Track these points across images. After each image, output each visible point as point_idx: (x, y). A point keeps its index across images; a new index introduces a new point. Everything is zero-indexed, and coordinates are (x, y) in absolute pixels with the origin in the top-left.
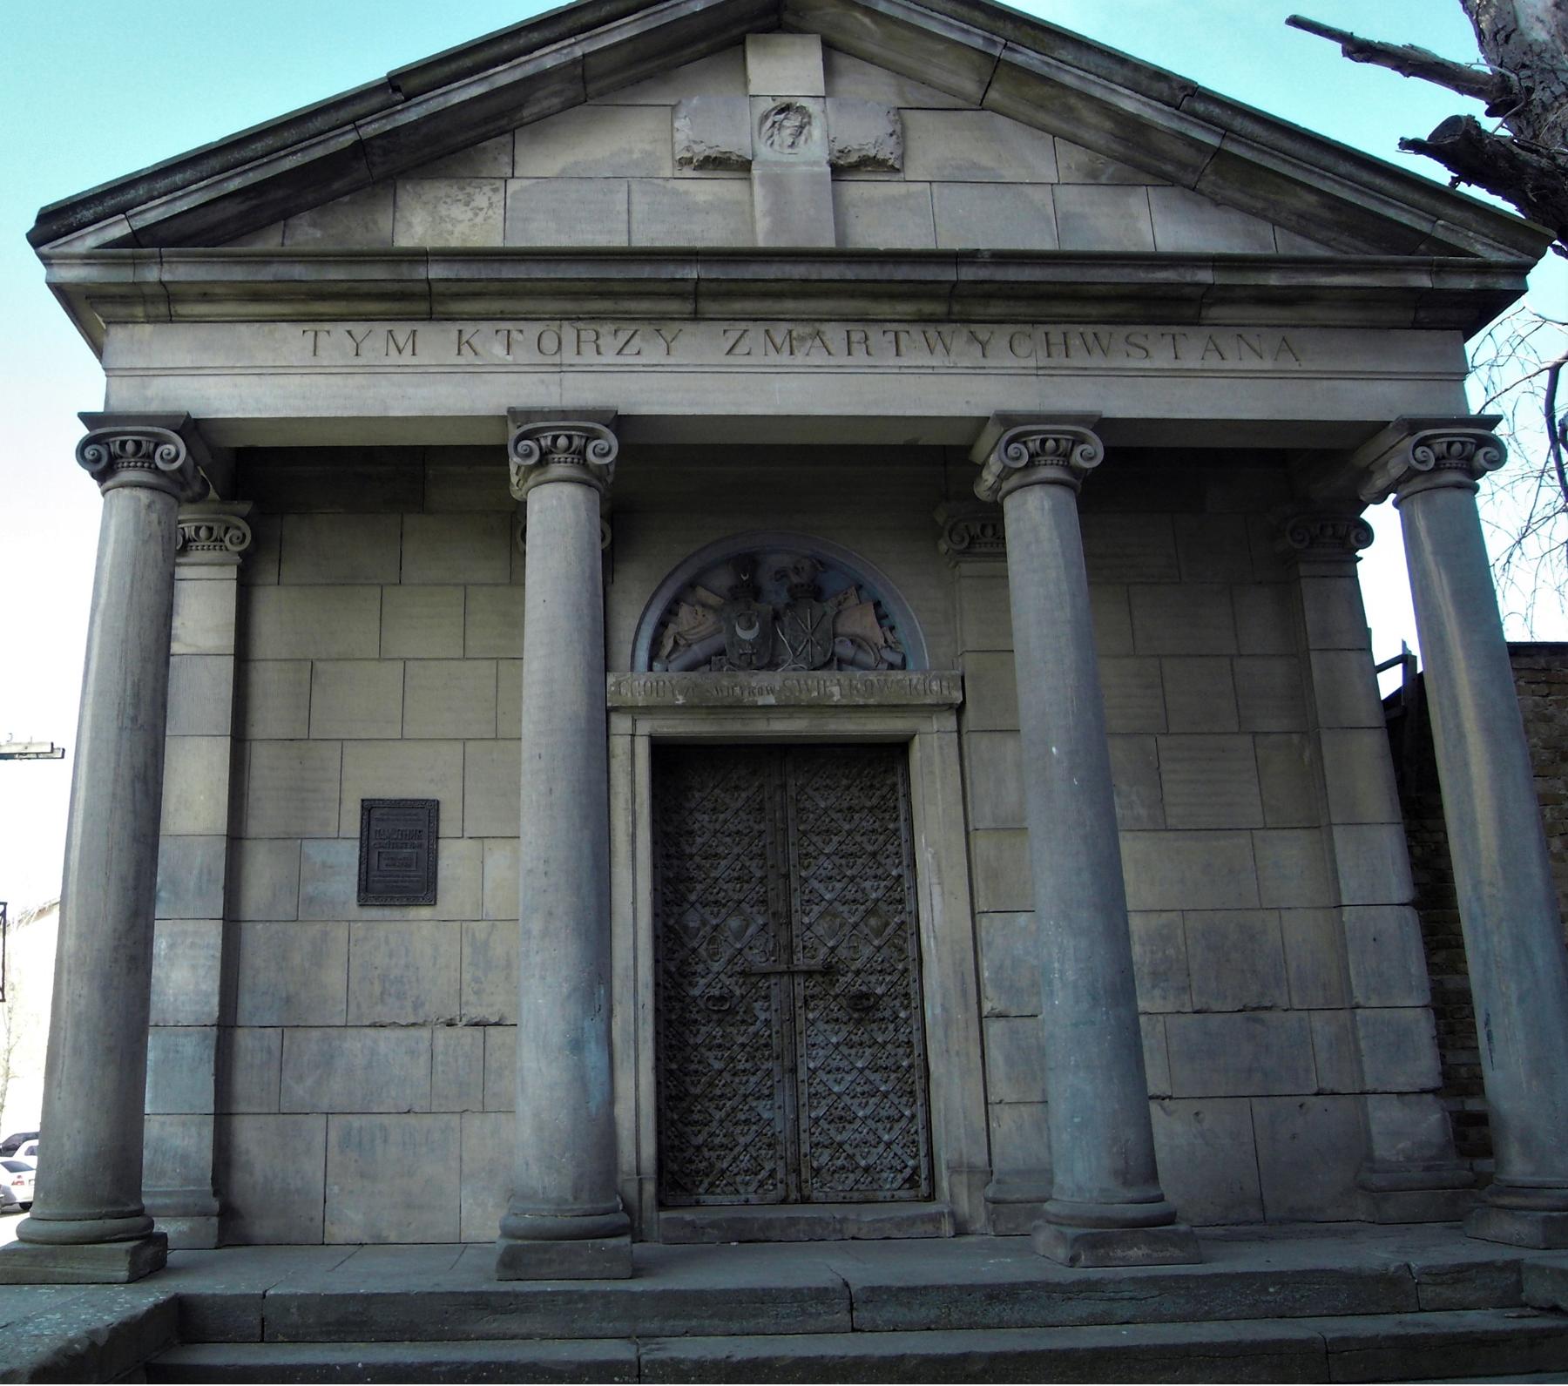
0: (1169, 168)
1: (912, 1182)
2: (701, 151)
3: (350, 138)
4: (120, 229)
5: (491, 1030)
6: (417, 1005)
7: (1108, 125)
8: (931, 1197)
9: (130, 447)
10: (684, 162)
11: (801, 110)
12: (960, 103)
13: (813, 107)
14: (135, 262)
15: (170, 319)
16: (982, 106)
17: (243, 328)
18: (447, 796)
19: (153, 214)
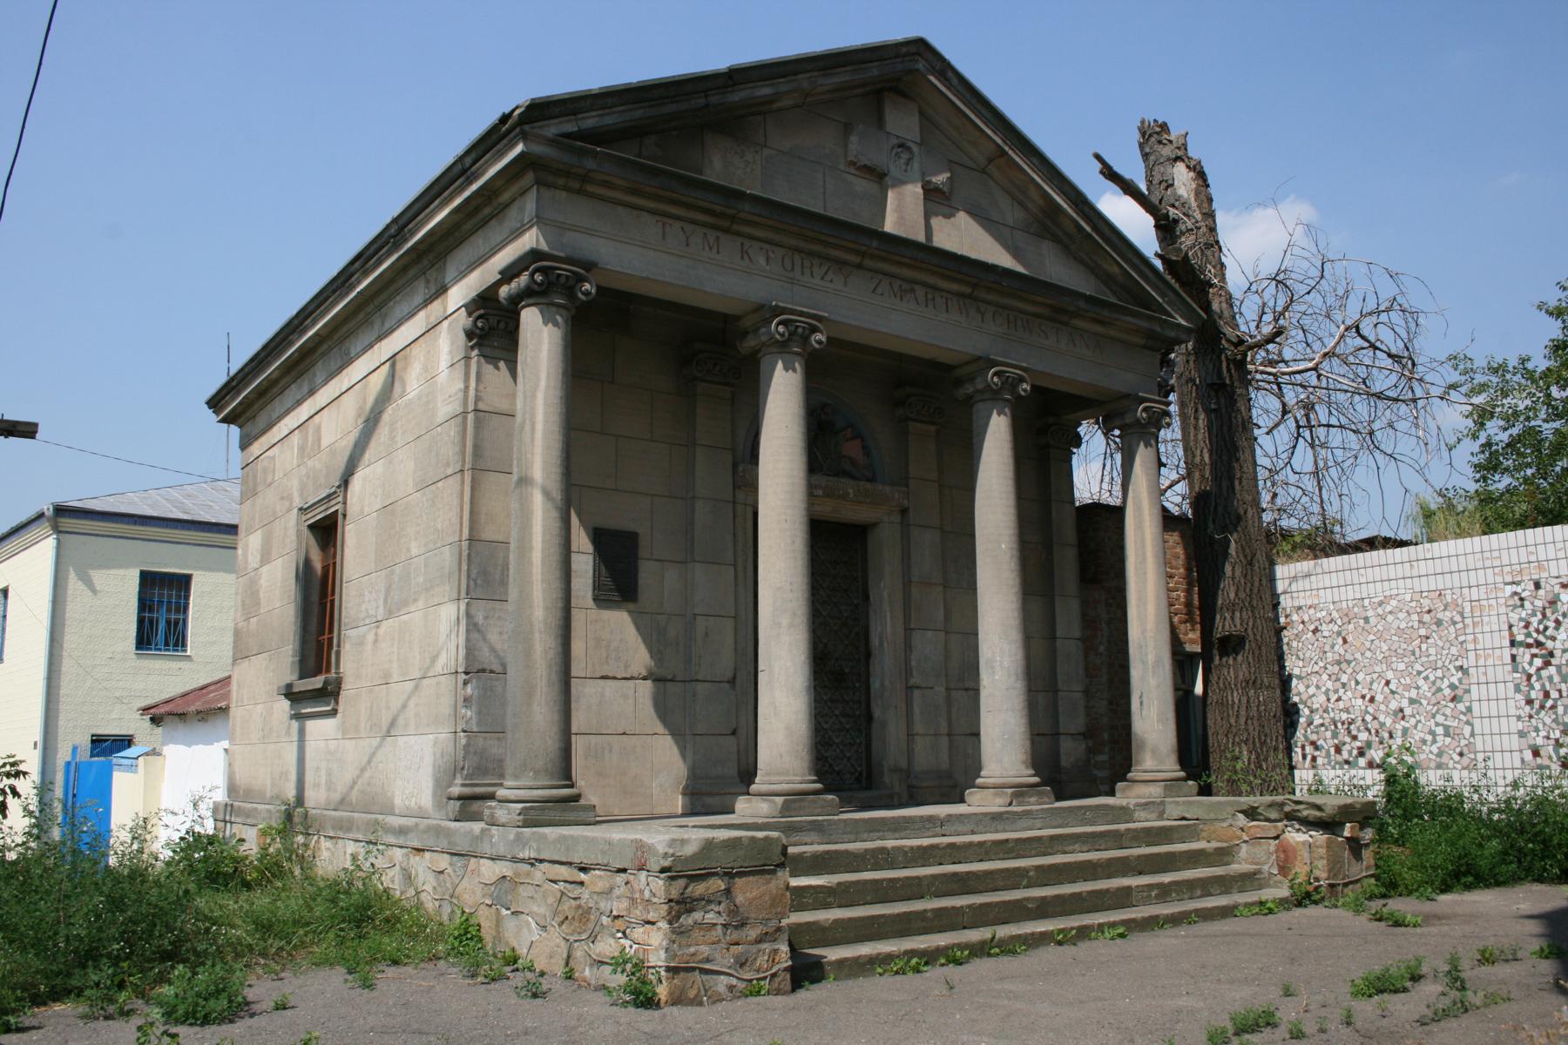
0: (1060, 233)
1: (858, 780)
2: (864, 161)
3: (702, 101)
4: (570, 127)
5: (669, 684)
6: (626, 667)
7: (1041, 202)
8: (869, 787)
9: (563, 280)
10: (853, 164)
11: (909, 149)
12: (971, 164)
13: (915, 149)
14: (582, 153)
15: (579, 192)
16: (983, 172)
17: (620, 209)
18: (640, 531)
19: (590, 121)
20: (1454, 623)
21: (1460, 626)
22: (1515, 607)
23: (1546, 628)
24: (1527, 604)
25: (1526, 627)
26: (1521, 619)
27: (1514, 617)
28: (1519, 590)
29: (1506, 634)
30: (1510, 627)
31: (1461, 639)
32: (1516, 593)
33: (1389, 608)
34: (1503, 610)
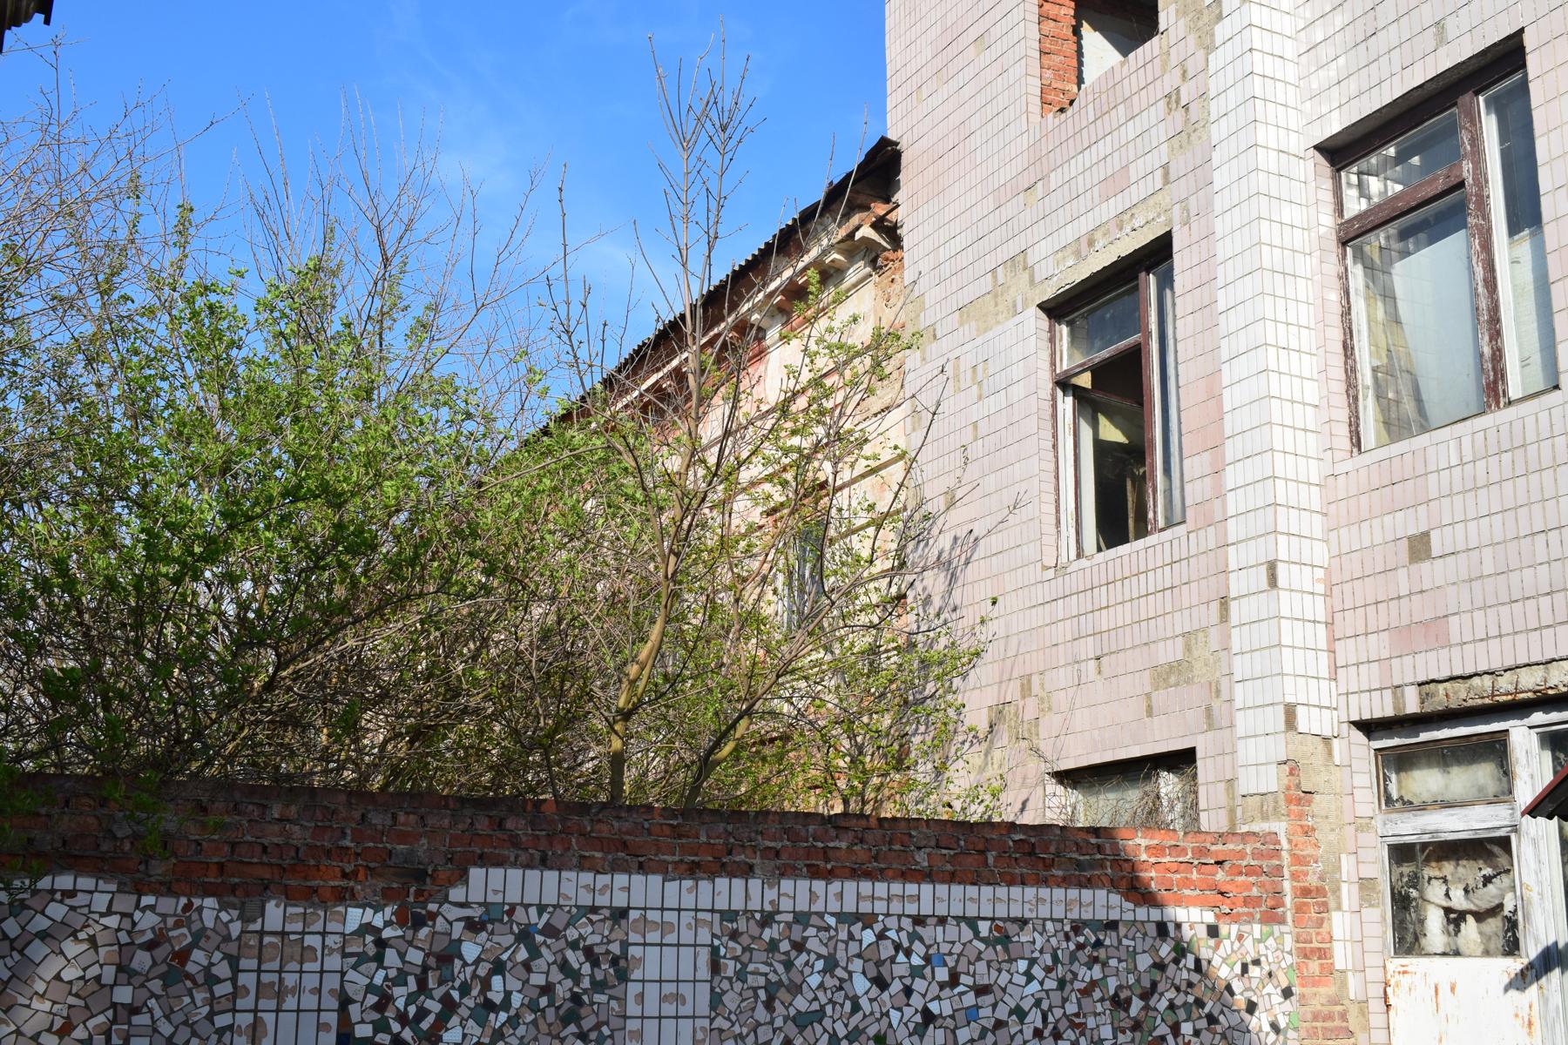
20: (211, 980)
21: (223, 989)
22: (362, 958)
23: (423, 1013)
24: (391, 957)
25: (380, 1007)
26: (370, 988)
27: (357, 980)
28: (378, 921)
29: (331, 1018)
30: (345, 1001)
31: (222, 1020)
32: (367, 928)
33: (41, 923)
34: (334, 962)
